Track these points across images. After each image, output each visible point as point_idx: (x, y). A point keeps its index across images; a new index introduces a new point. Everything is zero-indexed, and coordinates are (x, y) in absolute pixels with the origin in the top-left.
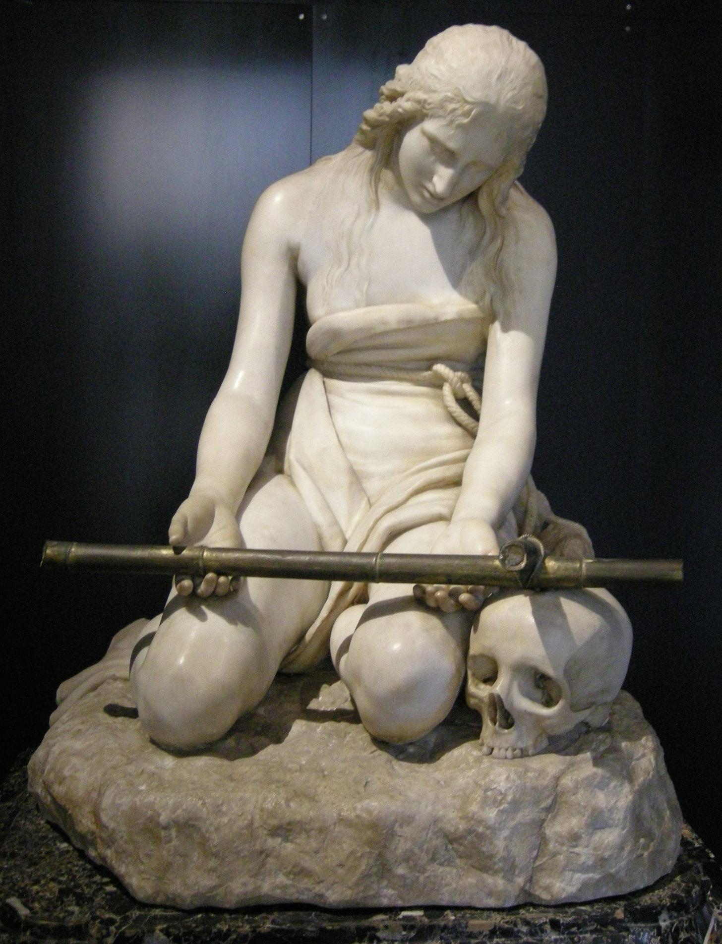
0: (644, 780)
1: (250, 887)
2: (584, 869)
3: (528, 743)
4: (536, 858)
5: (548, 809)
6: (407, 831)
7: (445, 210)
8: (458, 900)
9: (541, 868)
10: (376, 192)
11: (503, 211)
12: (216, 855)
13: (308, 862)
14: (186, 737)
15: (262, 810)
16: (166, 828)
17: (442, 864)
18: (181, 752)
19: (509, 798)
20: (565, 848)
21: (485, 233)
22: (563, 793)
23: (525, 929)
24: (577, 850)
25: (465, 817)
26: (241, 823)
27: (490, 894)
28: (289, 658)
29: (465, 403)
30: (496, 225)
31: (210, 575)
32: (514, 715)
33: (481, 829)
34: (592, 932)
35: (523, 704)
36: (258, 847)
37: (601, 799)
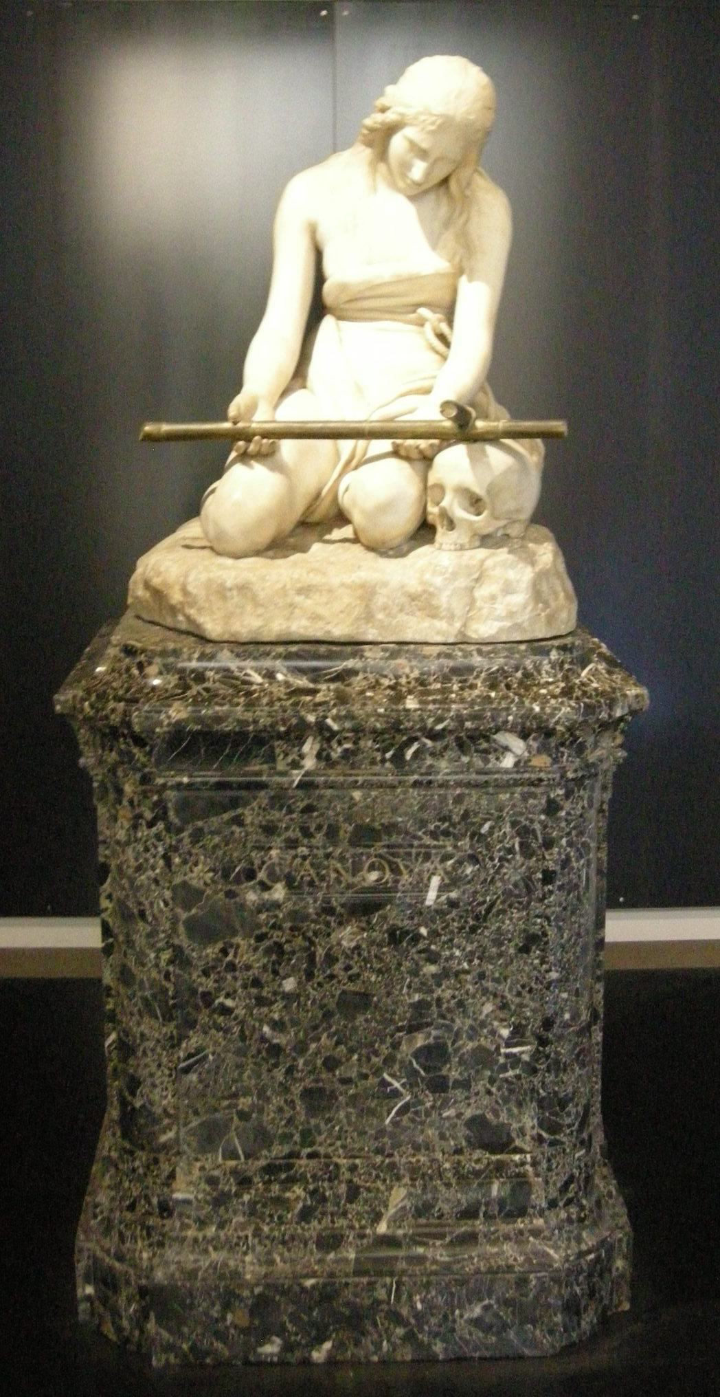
1: (284, 627)
2: (499, 619)
3: (465, 540)
4: (469, 611)
5: (477, 580)
6: (384, 591)
7: (426, 192)
8: (418, 638)
9: (471, 618)
11: (468, 193)
12: (262, 605)
13: (322, 611)
14: (241, 544)
16: (230, 589)
17: (407, 614)
18: (237, 556)
19: (450, 570)
20: (487, 605)
21: (455, 209)
22: (486, 570)
23: (460, 654)
24: (496, 606)
25: (422, 583)
26: (279, 586)
27: (438, 633)
28: (310, 509)
31: (257, 438)
32: (456, 521)
33: (431, 590)
34: (505, 657)
35: (460, 513)
36: (289, 600)
37: (512, 575)
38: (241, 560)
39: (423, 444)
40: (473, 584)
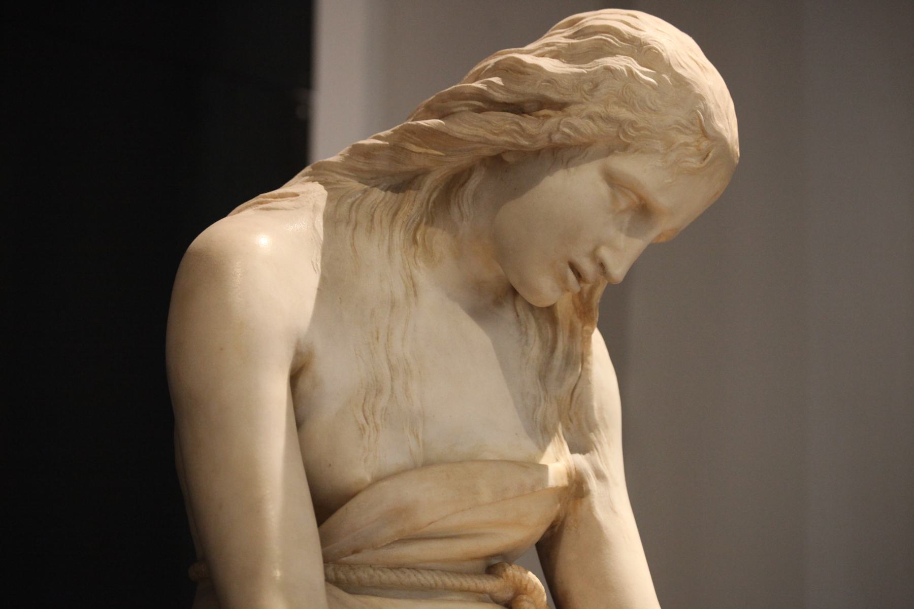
21: (553, 350)
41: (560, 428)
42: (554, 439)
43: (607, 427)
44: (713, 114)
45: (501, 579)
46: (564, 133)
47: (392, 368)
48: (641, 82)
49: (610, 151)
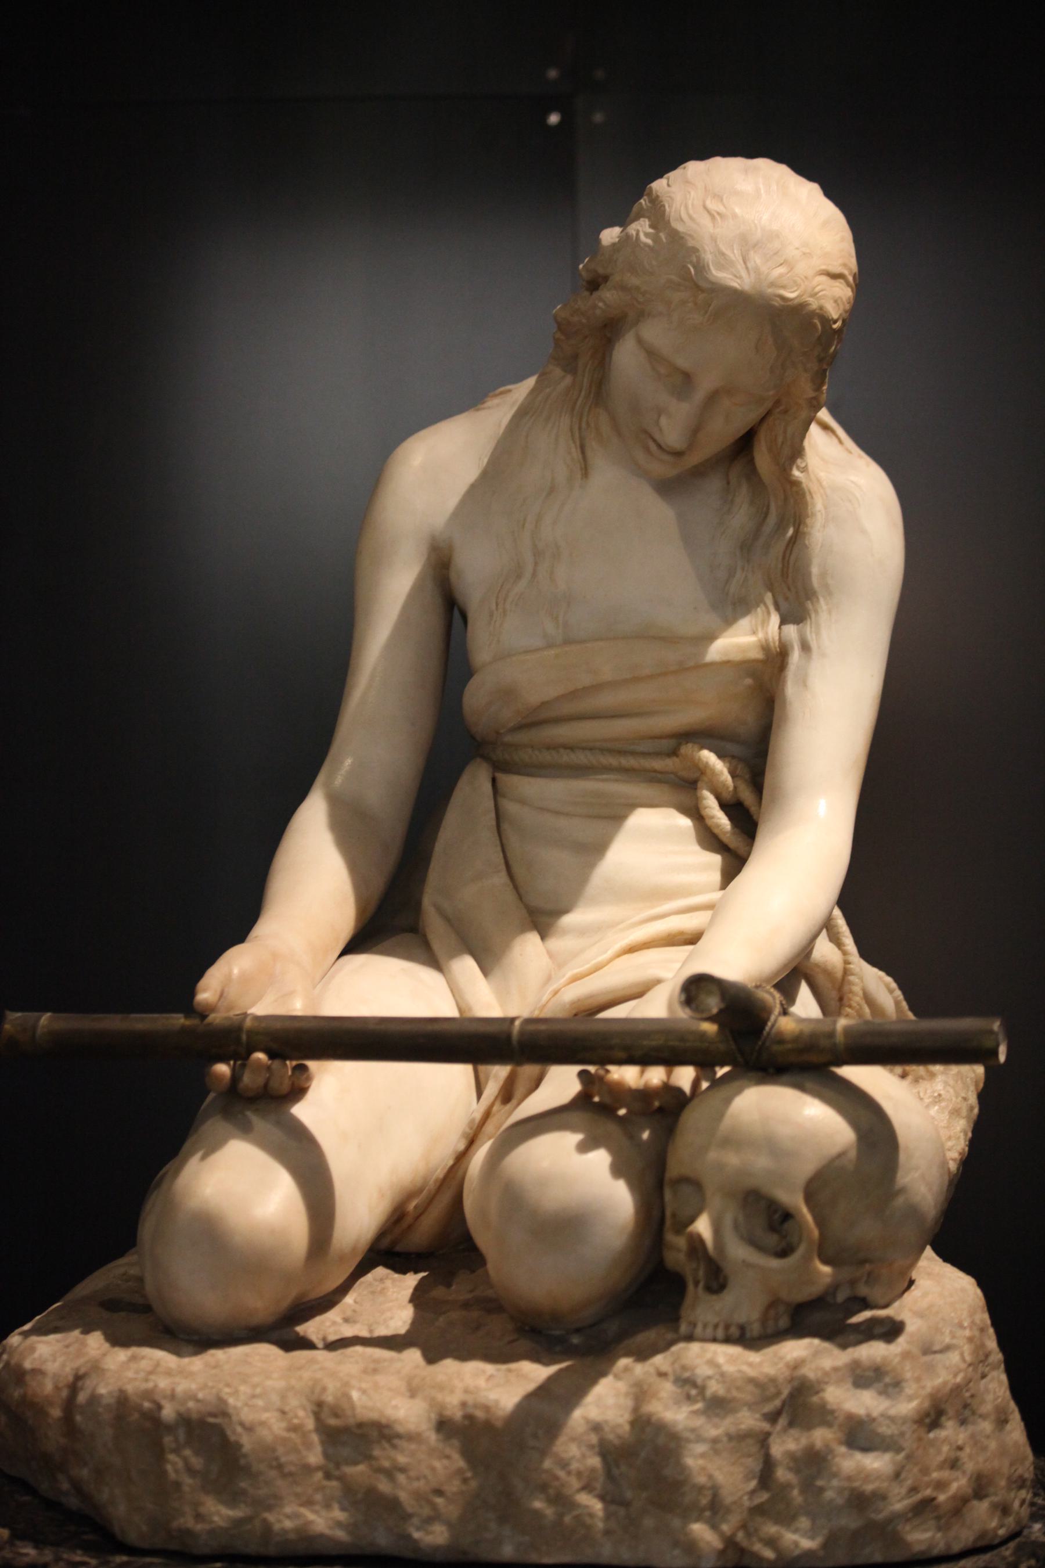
0: (945, 1383)
4: (753, 1493)
7: (699, 472)
10: (583, 449)
15: (320, 1405)
16: (170, 1428)
29: (733, 808)
30: (786, 499)
35: (738, 1252)
38: (218, 1355)
39: (656, 1075)
40: (766, 1426)
41: (769, 598)
42: (756, 610)
43: (830, 593)
44: (708, 266)
45: (675, 759)
46: (600, 308)
47: (537, 554)
48: (642, 245)
49: (637, 322)
